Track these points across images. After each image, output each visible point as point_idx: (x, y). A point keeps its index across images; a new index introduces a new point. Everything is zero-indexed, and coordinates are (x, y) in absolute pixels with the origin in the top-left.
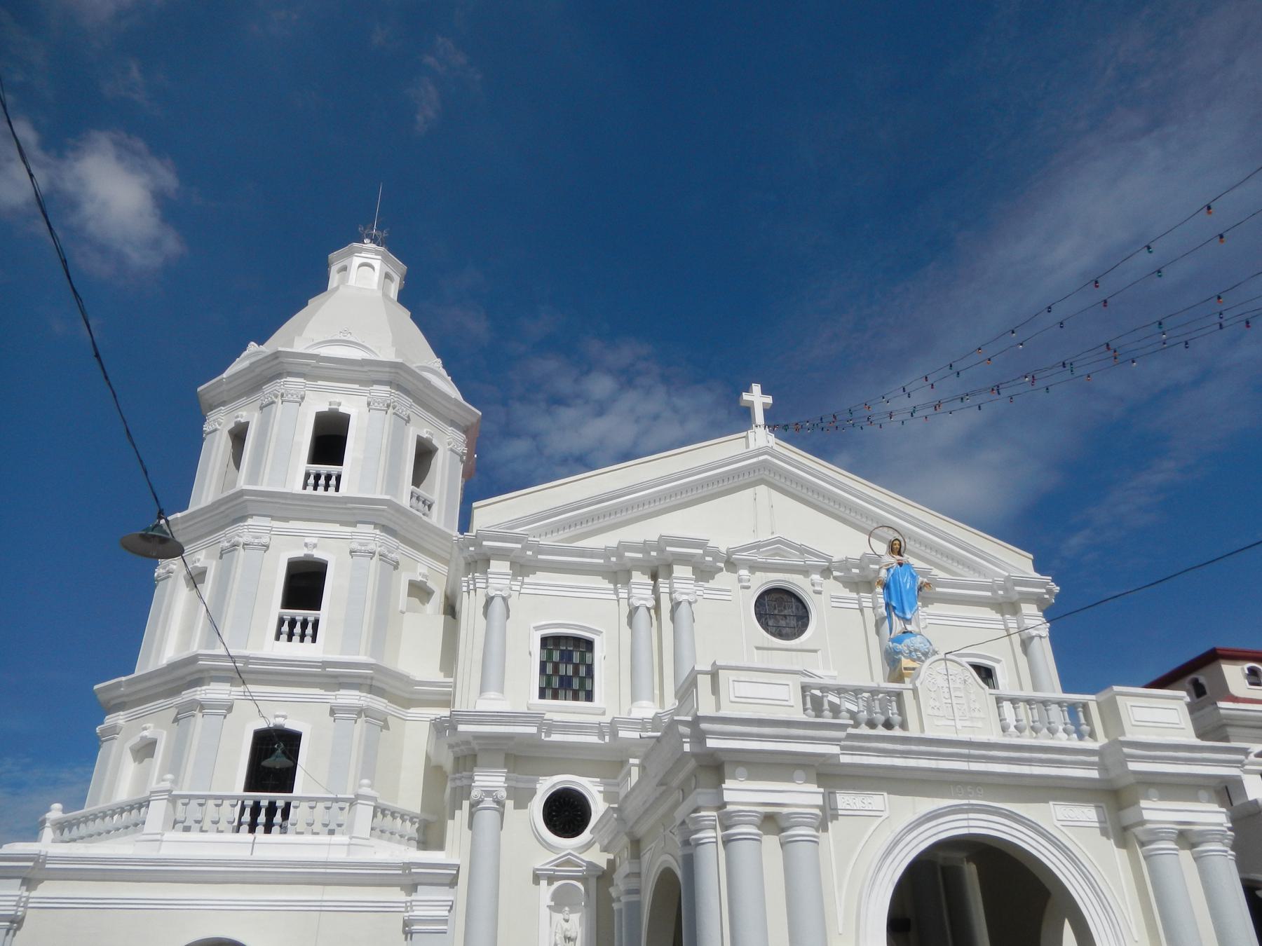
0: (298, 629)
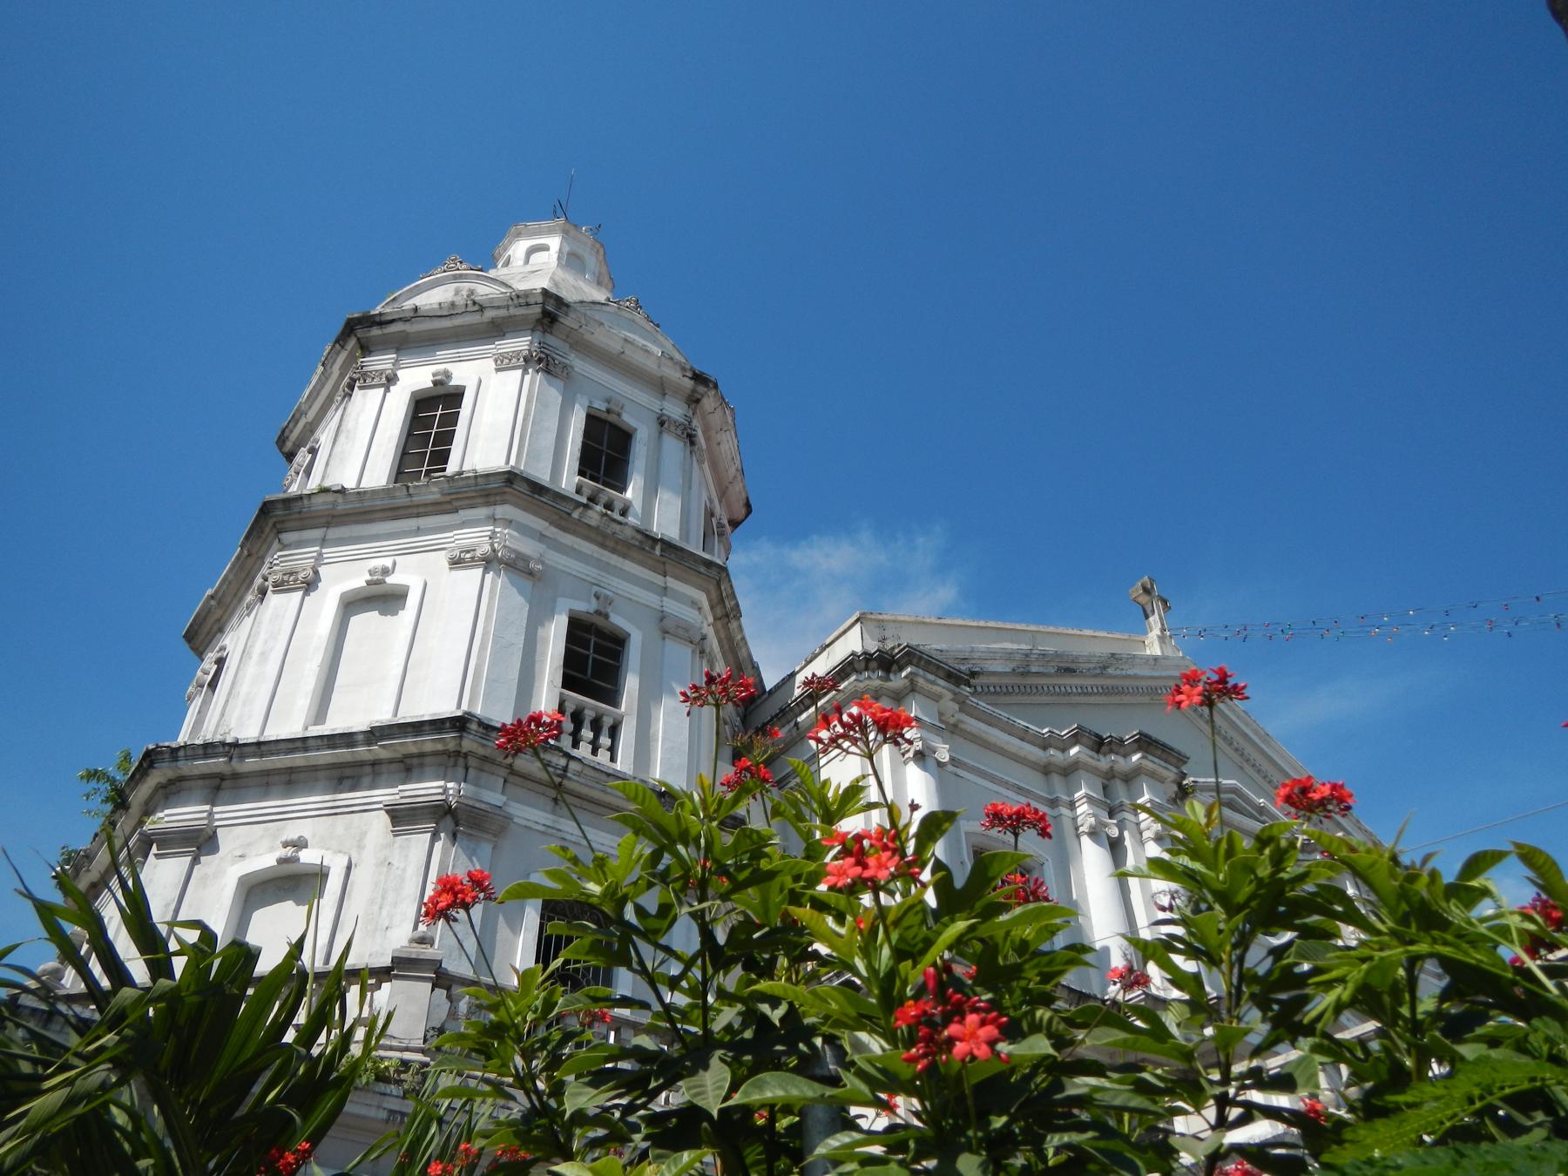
0: (587, 733)
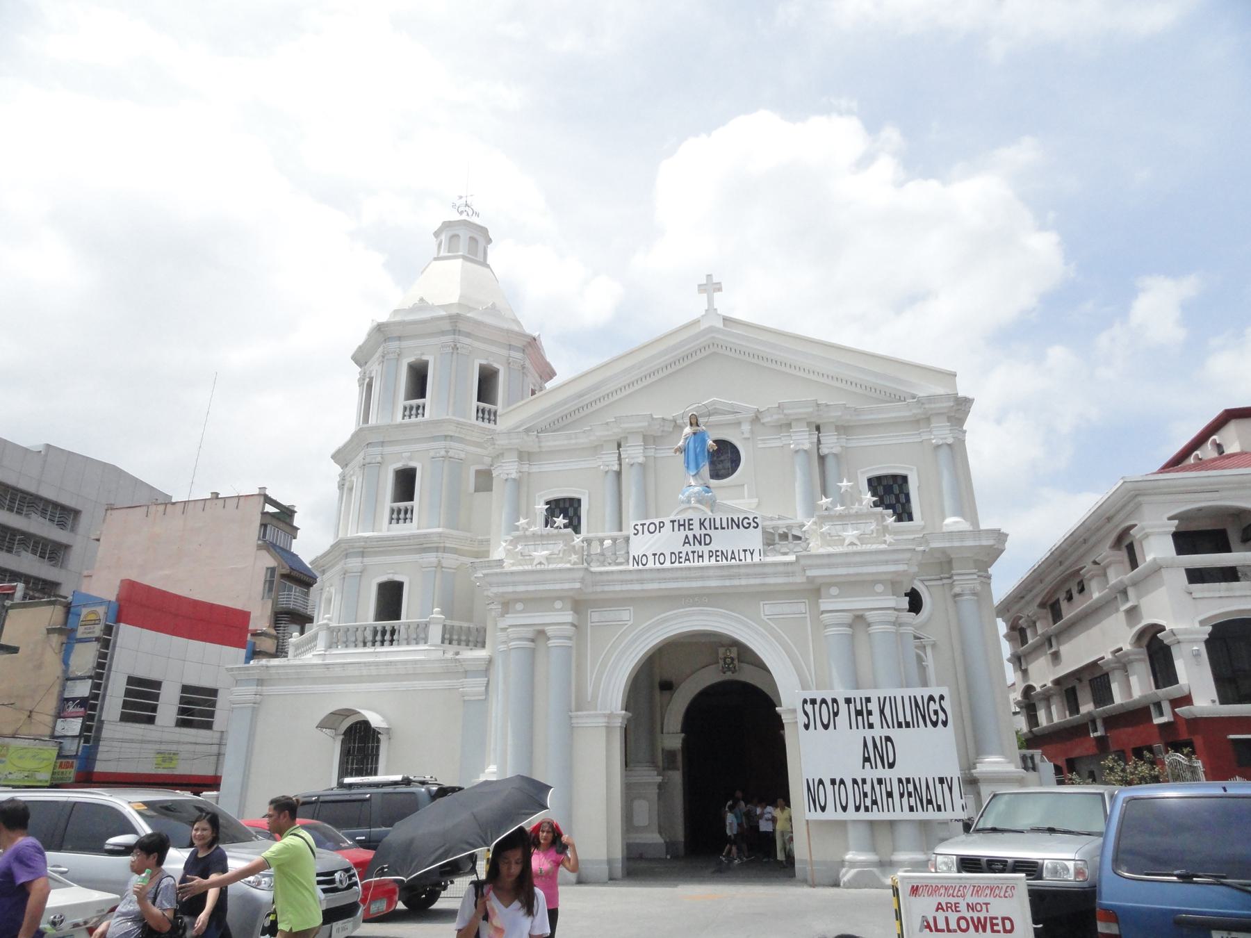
0: (402, 516)
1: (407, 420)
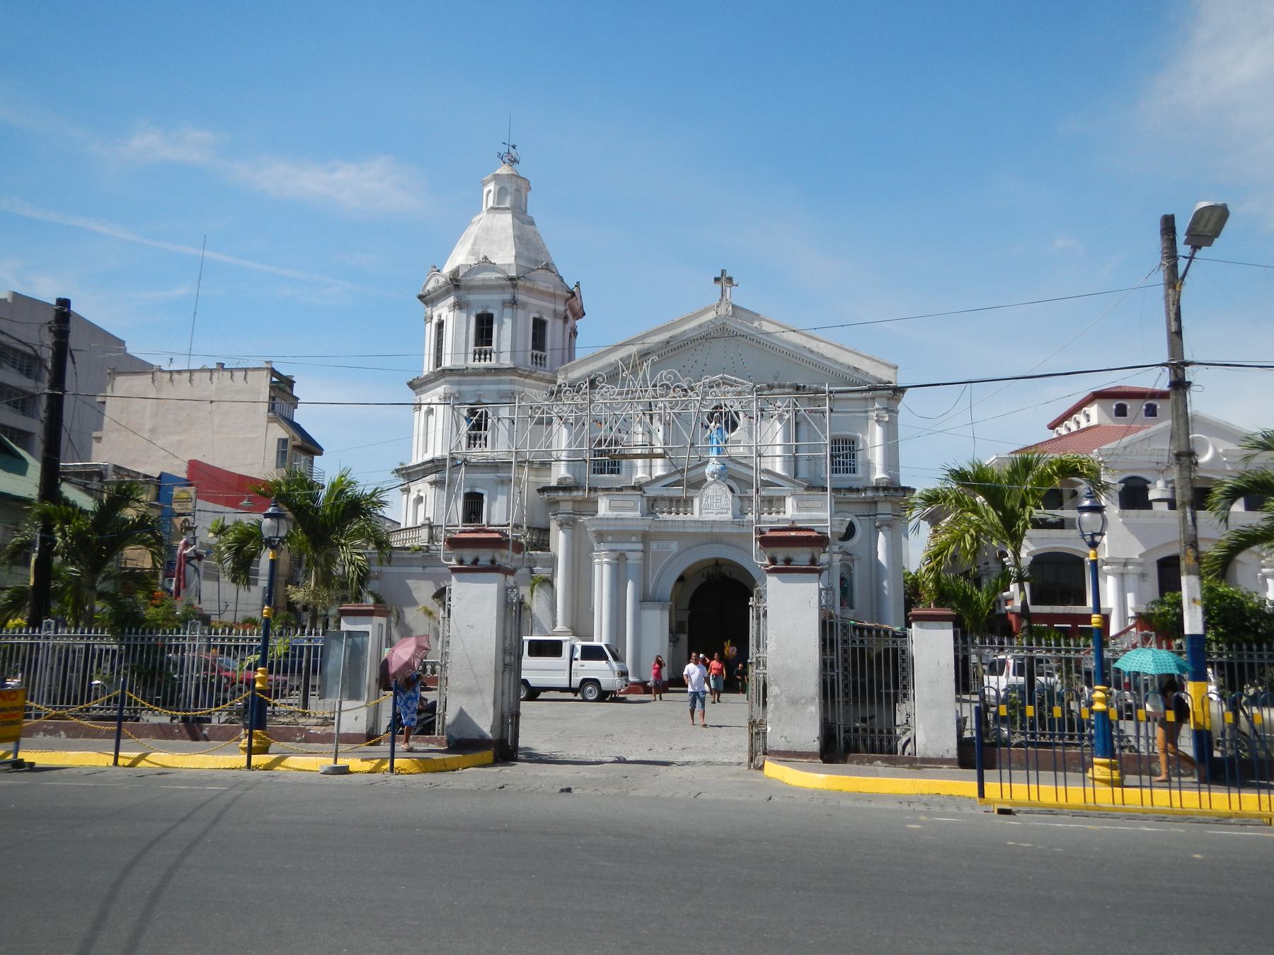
1: (477, 362)
